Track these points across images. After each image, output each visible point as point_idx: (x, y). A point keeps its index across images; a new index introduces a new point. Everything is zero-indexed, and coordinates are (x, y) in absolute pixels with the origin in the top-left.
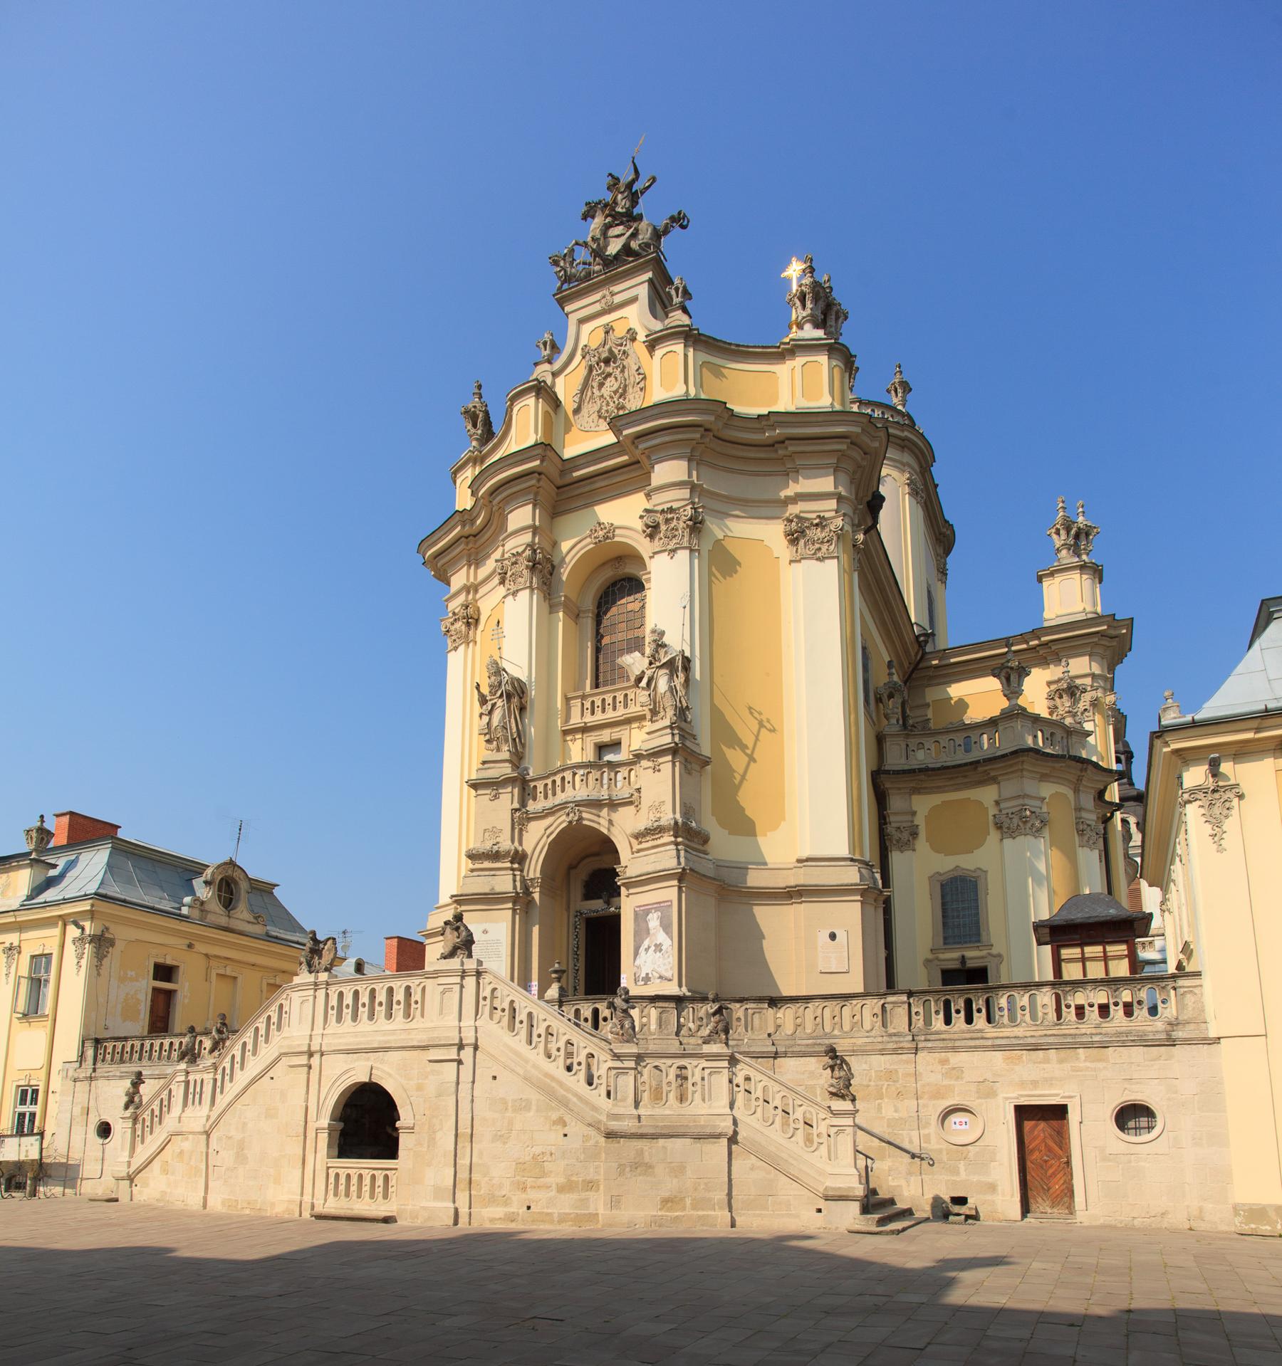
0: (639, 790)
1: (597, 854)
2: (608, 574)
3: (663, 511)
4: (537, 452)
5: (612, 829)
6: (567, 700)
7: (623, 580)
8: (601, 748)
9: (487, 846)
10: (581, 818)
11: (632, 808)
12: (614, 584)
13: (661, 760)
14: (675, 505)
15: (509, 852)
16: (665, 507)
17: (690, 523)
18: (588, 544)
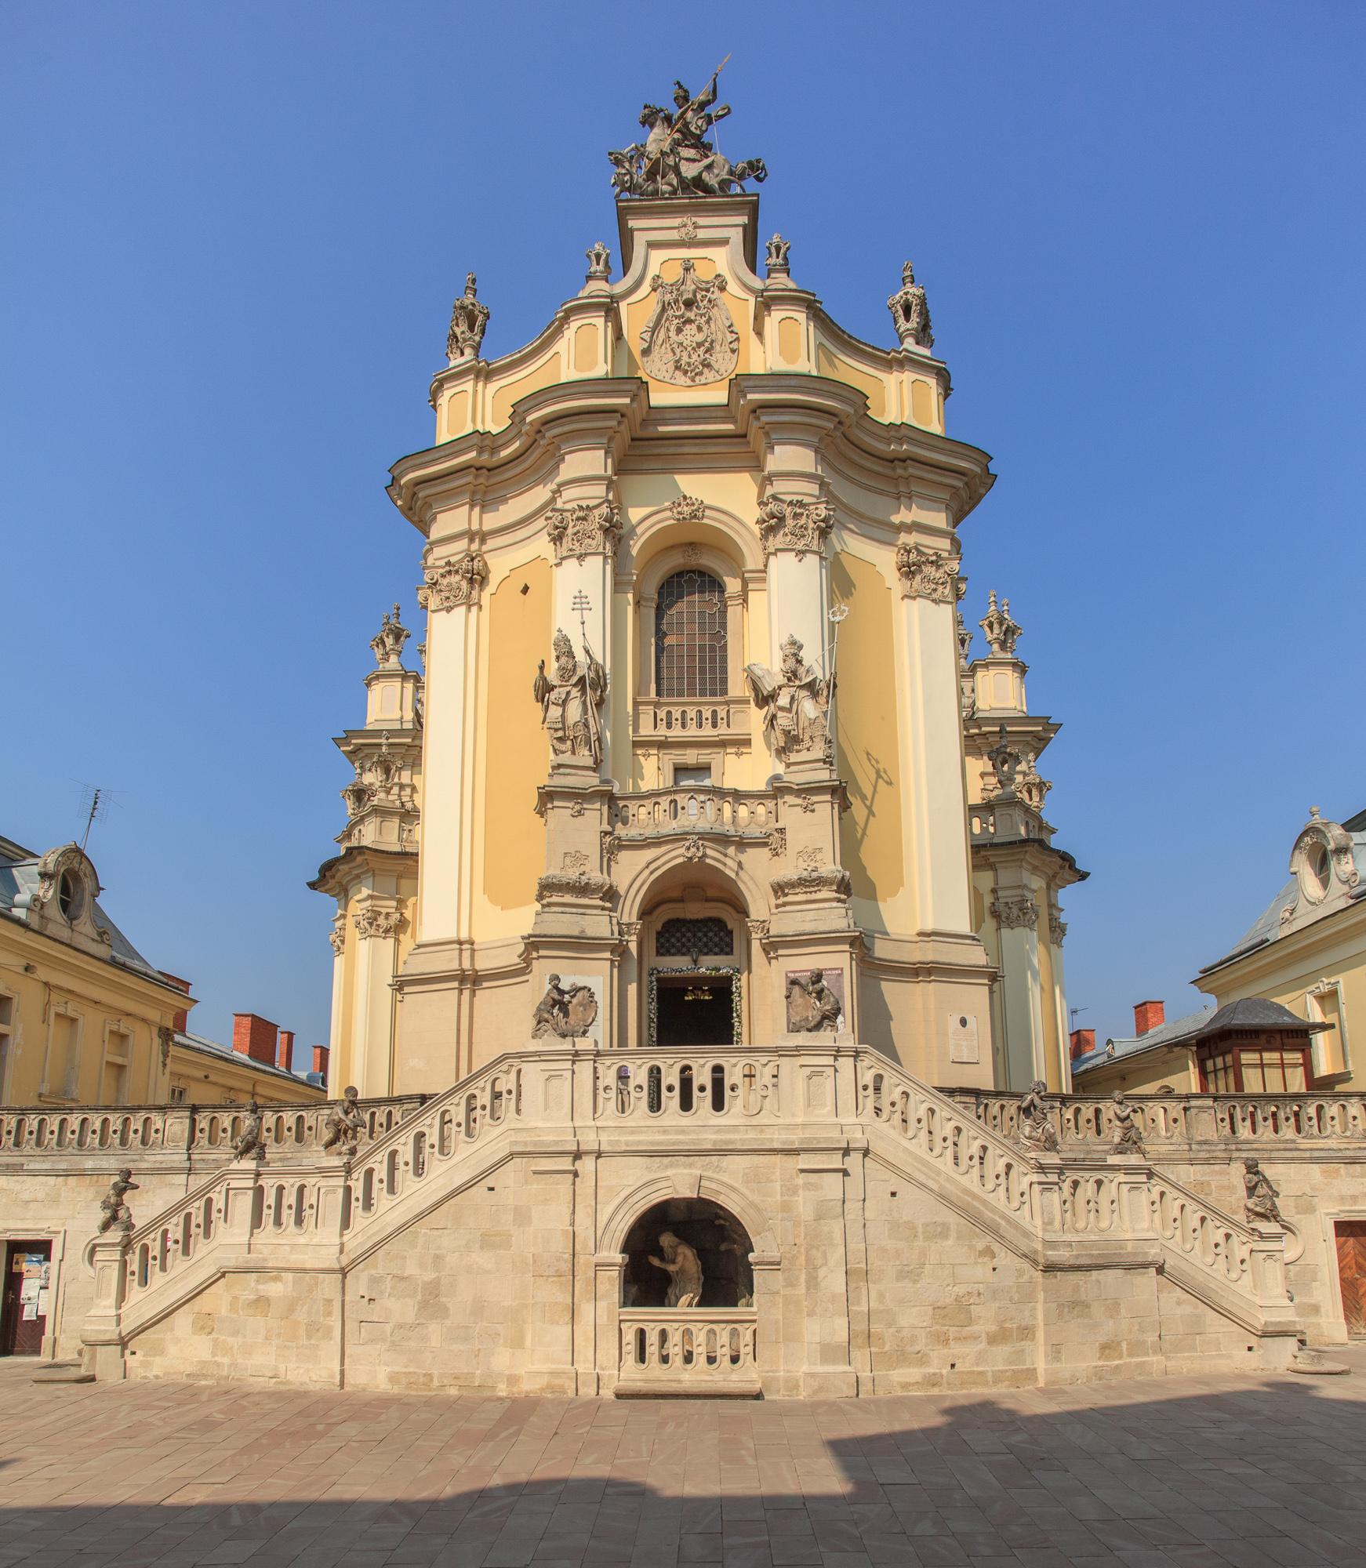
0: (782, 831)
1: (681, 900)
2: (676, 561)
3: (791, 503)
4: (628, 387)
5: (741, 873)
6: (636, 704)
7: (693, 572)
8: (680, 770)
9: (572, 875)
10: (705, 855)
11: (765, 852)
12: (680, 574)
13: (815, 799)
14: (807, 500)
15: (602, 886)
16: (796, 498)
17: (823, 525)
18: (666, 519)
